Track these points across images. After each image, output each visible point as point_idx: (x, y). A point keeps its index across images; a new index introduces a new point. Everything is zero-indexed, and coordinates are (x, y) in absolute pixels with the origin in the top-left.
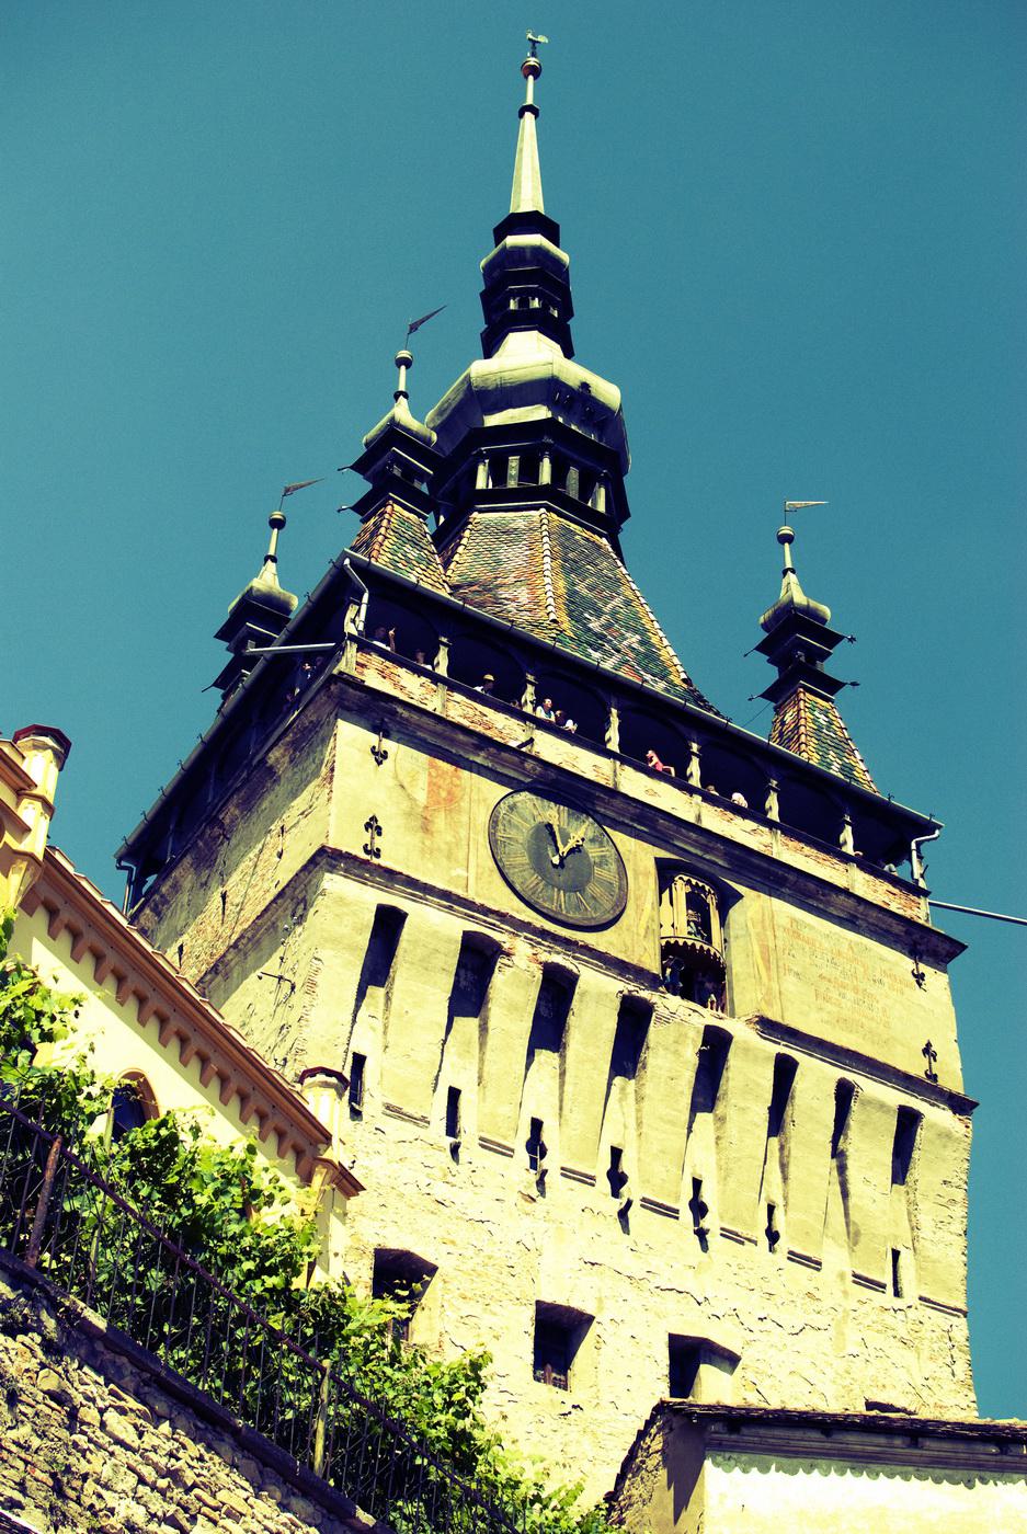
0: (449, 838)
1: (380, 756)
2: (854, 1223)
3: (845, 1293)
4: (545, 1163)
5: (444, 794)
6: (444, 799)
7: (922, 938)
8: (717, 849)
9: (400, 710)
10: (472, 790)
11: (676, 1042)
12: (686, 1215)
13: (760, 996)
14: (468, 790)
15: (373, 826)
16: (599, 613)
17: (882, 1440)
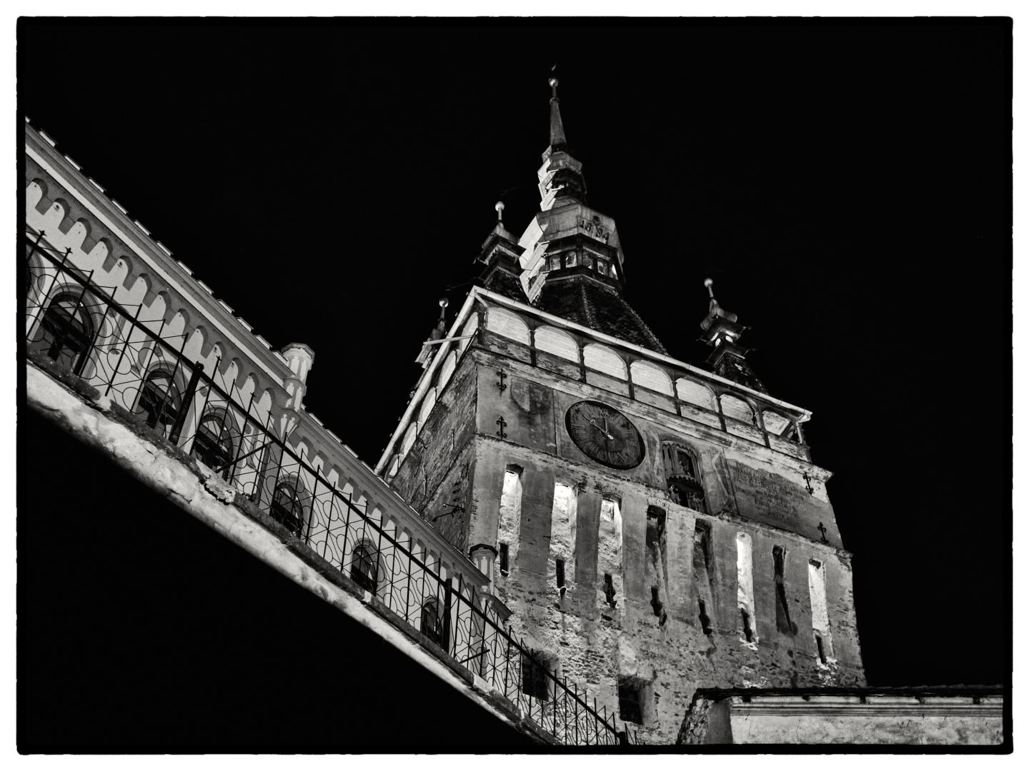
0: (544, 427)
1: (502, 387)
2: (793, 623)
3: (794, 663)
4: (615, 598)
5: (539, 405)
6: (540, 408)
7: (809, 469)
8: (692, 428)
9: (511, 362)
10: (554, 403)
11: (681, 528)
12: (699, 624)
13: (725, 503)
14: (552, 403)
15: (501, 422)
16: (614, 323)
17: (841, 700)
